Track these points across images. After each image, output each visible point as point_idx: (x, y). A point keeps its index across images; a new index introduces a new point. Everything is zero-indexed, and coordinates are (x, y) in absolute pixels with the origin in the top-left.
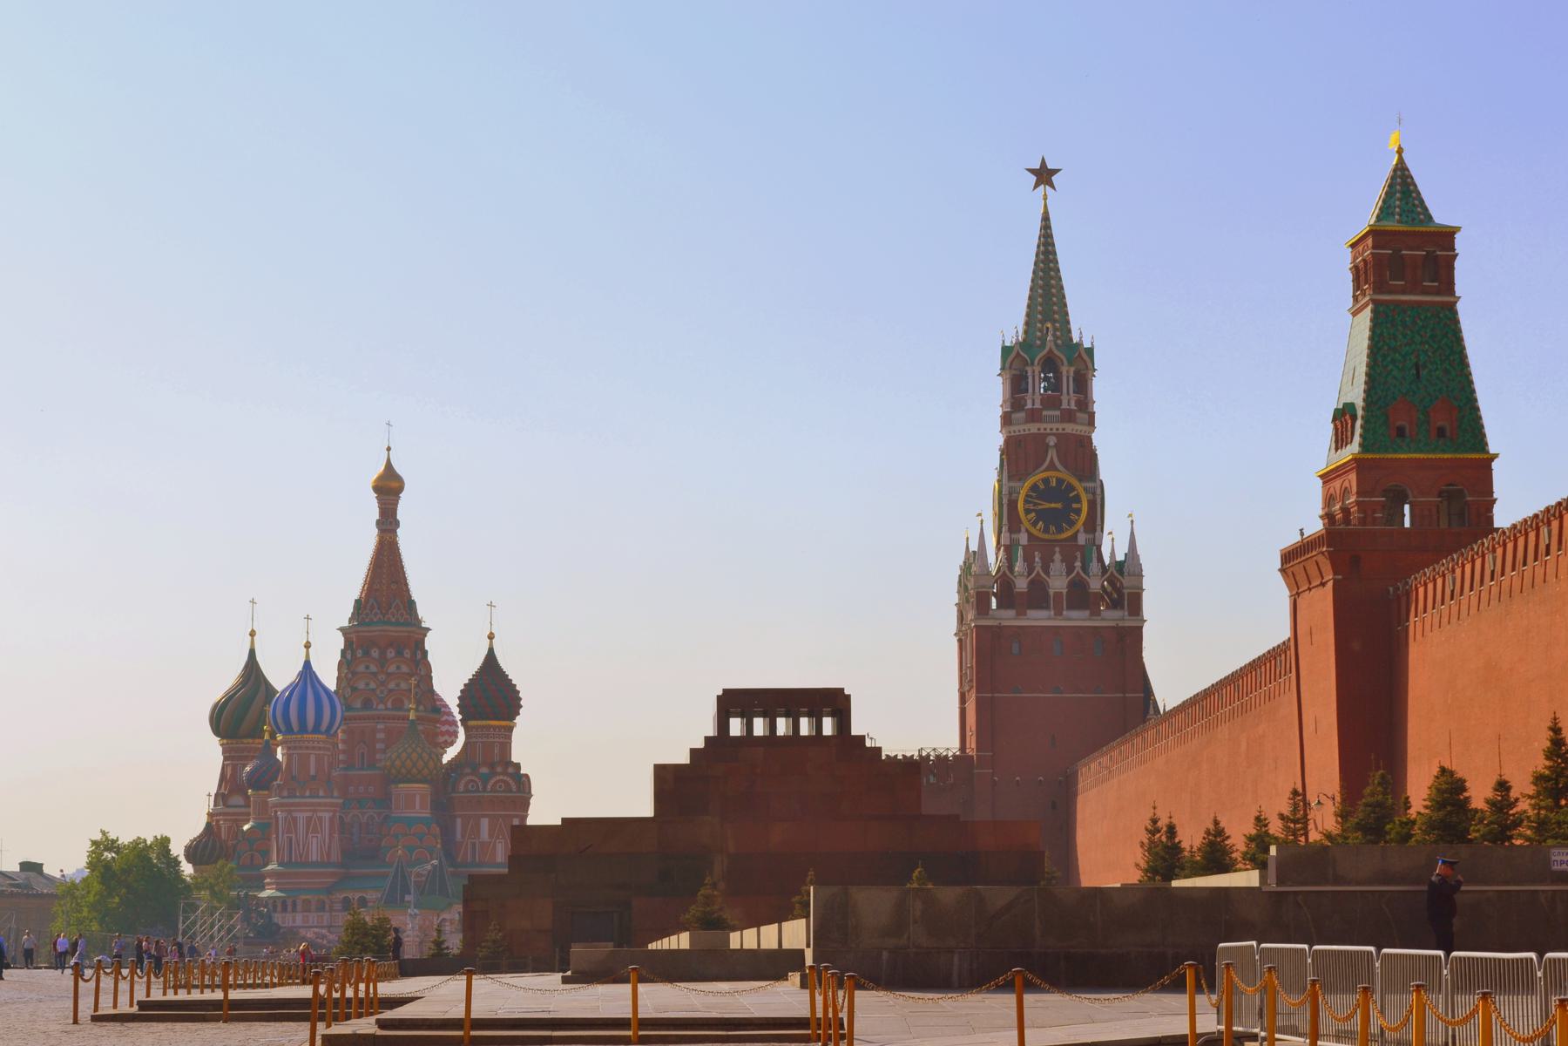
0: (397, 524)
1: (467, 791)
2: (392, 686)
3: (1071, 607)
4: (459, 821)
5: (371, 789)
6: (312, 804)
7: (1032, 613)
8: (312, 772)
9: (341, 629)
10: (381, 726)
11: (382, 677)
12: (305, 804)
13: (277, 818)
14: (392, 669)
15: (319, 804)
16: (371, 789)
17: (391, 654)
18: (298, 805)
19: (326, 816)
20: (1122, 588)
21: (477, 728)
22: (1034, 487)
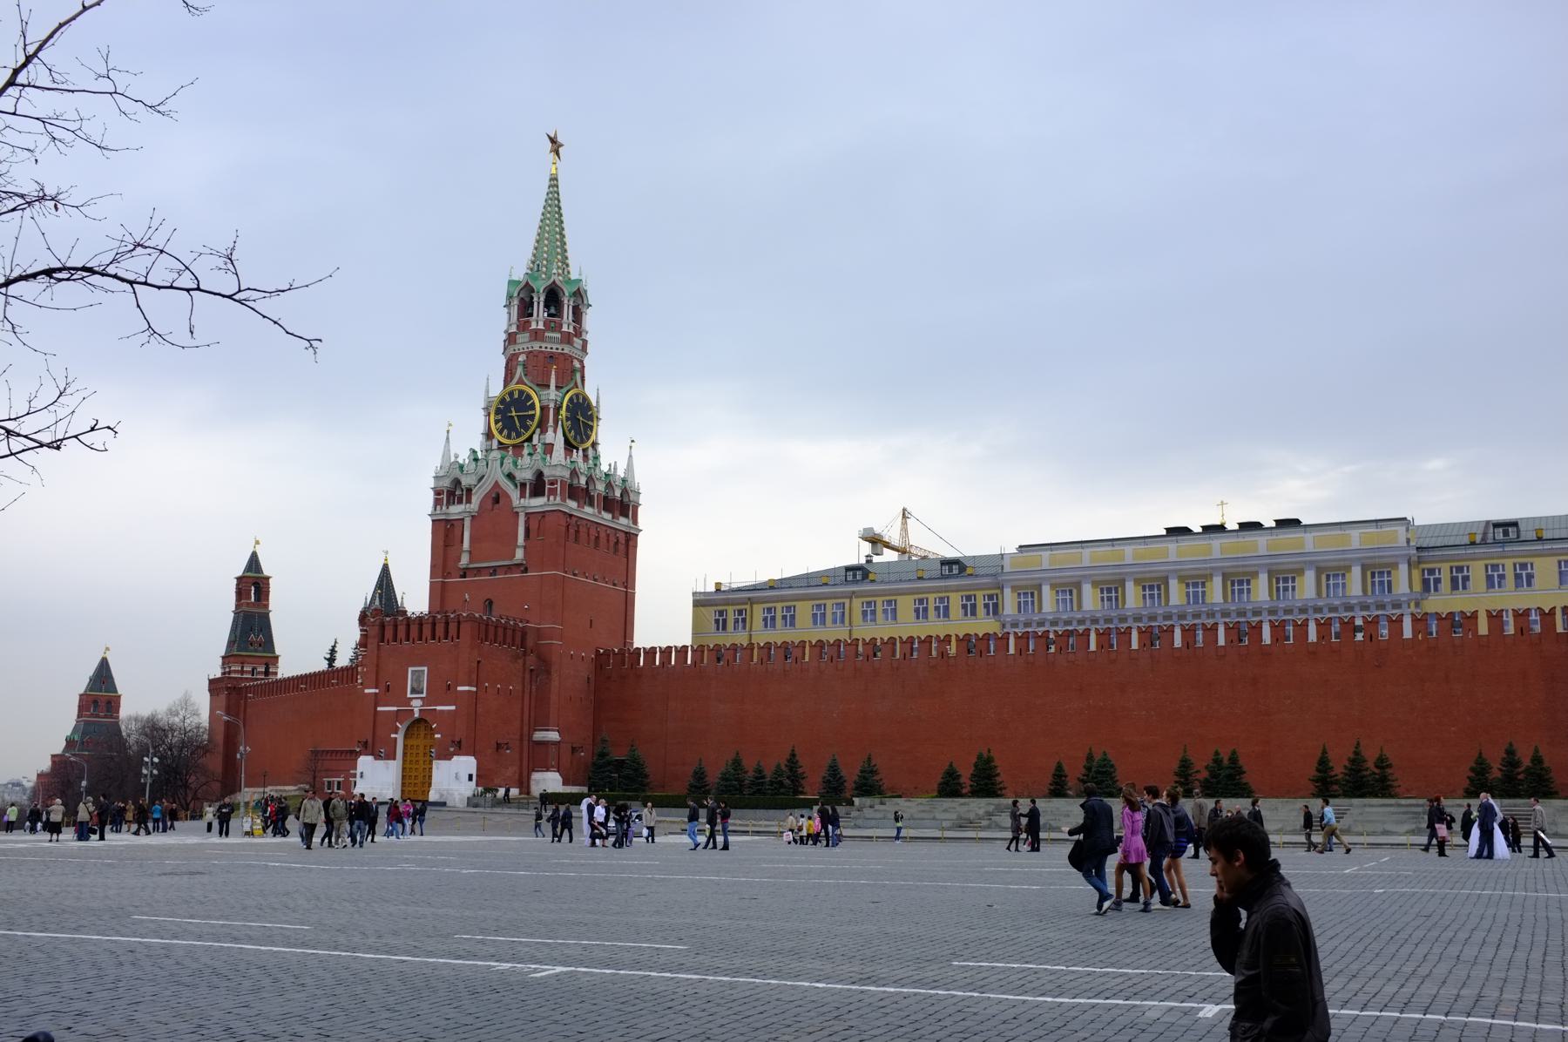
3: (606, 509)
7: (588, 509)
20: (622, 503)
22: (571, 399)
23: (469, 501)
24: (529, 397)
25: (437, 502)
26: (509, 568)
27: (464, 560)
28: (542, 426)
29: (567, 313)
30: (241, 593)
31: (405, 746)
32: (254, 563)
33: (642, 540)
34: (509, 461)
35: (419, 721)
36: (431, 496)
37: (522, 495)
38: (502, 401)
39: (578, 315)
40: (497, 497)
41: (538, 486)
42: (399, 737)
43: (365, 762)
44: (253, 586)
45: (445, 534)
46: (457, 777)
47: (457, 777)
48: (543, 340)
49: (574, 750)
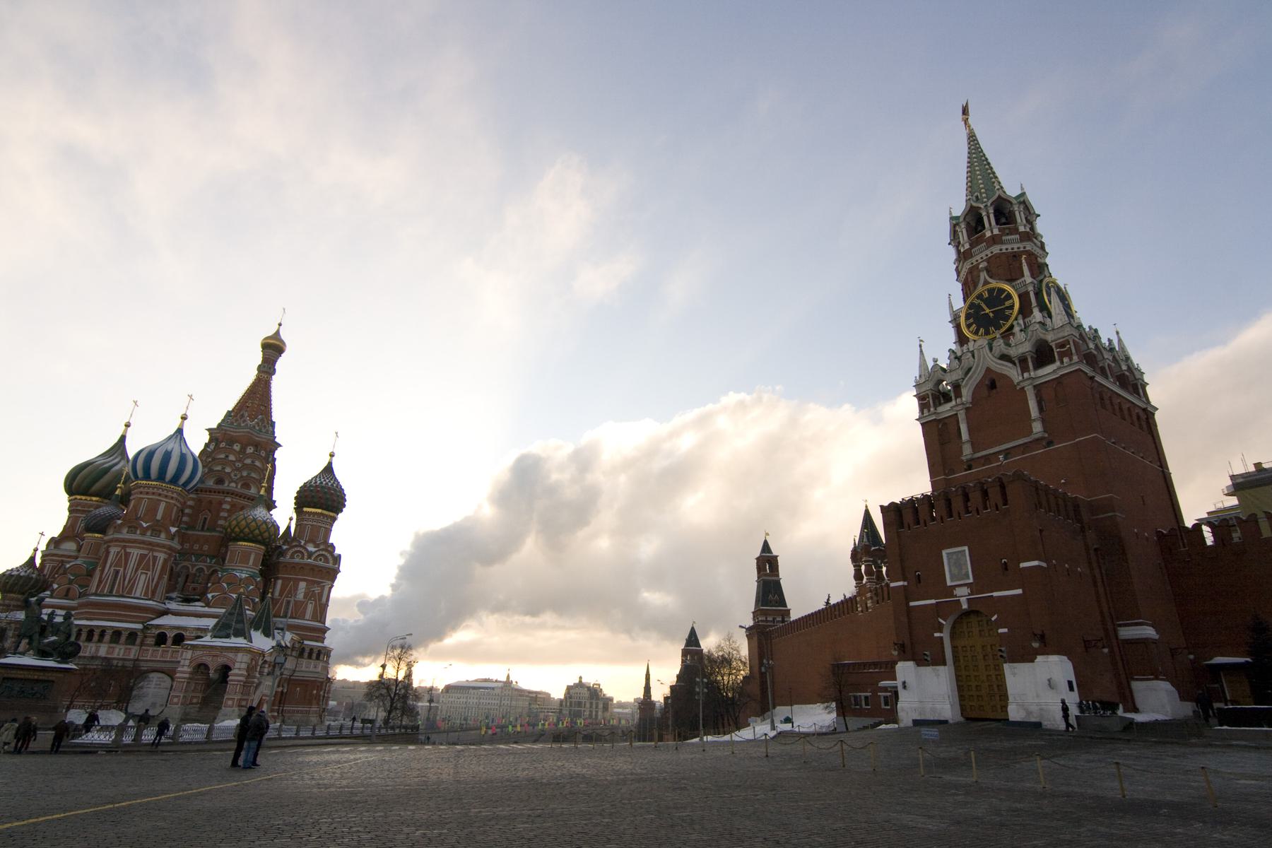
0: (274, 372)
1: (292, 557)
2: (245, 474)
4: (280, 582)
5: (206, 547)
6: (150, 544)
8: (159, 517)
9: (208, 430)
10: (228, 499)
11: (239, 465)
12: (143, 542)
13: (108, 553)
14: (248, 461)
15: (158, 545)
16: (206, 547)
17: (250, 450)
18: (135, 541)
19: (161, 556)
21: (310, 513)
23: (958, 395)
24: (1002, 291)
25: (923, 406)
26: (1025, 447)
27: (967, 451)
28: (1025, 311)
29: (1020, 218)
30: (760, 568)
31: (954, 648)
32: (766, 547)
33: (1158, 416)
34: (999, 345)
35: (967, 614)
36: (916, 400)
37: (1025, 369)
38: (972, 306)
39: (1030, 223)
40: (992, 382)
41: (1043, 354)
42: (945, 635)
43: (905, 670)
44: (767, 563)
45: (939, 437)
46: (1051, 684)
47: (1051, 684)
48: (1002, 243)
49: (1173, 652)
